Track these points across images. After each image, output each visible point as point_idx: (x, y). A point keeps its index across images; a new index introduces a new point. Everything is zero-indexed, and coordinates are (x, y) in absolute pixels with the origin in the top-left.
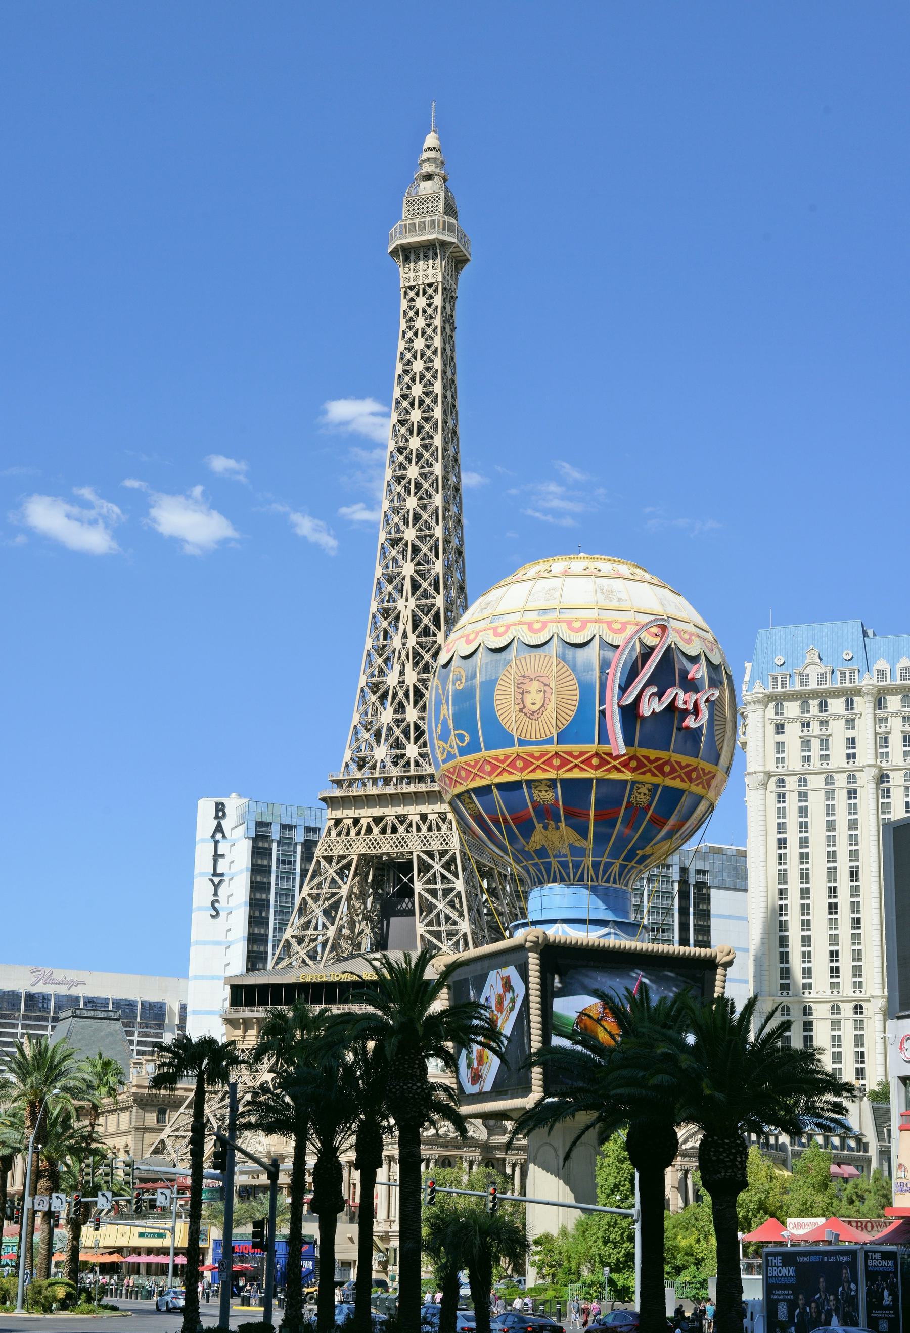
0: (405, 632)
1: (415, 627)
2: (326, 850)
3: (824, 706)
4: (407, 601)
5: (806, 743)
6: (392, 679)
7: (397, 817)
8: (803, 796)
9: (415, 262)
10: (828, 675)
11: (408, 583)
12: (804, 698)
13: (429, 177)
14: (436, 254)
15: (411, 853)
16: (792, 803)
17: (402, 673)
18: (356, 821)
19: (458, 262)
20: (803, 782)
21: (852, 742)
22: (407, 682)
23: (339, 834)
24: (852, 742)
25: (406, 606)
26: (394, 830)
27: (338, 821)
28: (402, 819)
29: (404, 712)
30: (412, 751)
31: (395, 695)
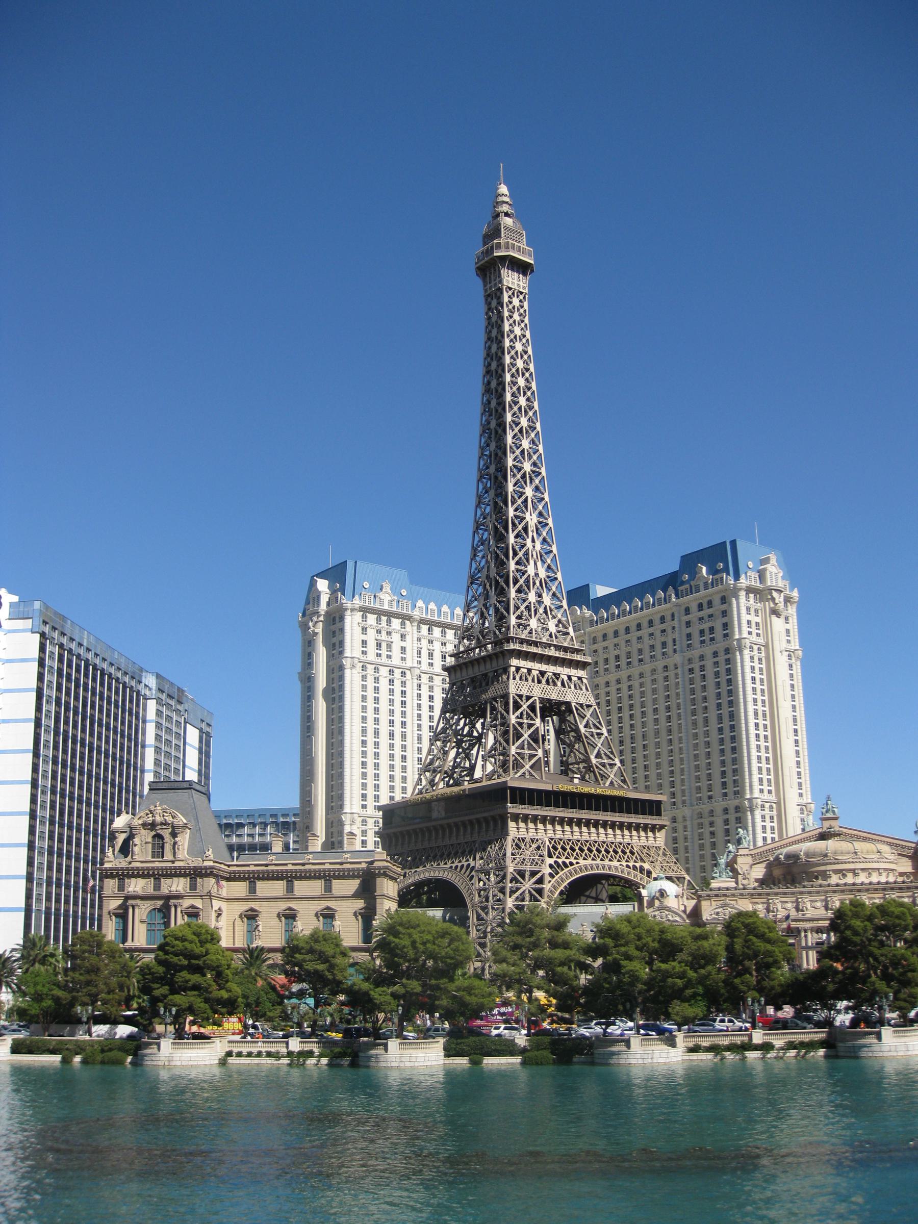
3: (389, 622)
5: (379, 645)
6: (531, 570)
7: (554, 674)
8: (376, 680)
10: (395, 603)
12: (379, 613)
13: (507, 214)
15: (568, 704)
16: (370, 684)
18: (529, 671)
20: (376, 670)
21: (403, 649)
24: (403, 649)
26: (555, 684)
28: (557, 676)
31: (534, 584)
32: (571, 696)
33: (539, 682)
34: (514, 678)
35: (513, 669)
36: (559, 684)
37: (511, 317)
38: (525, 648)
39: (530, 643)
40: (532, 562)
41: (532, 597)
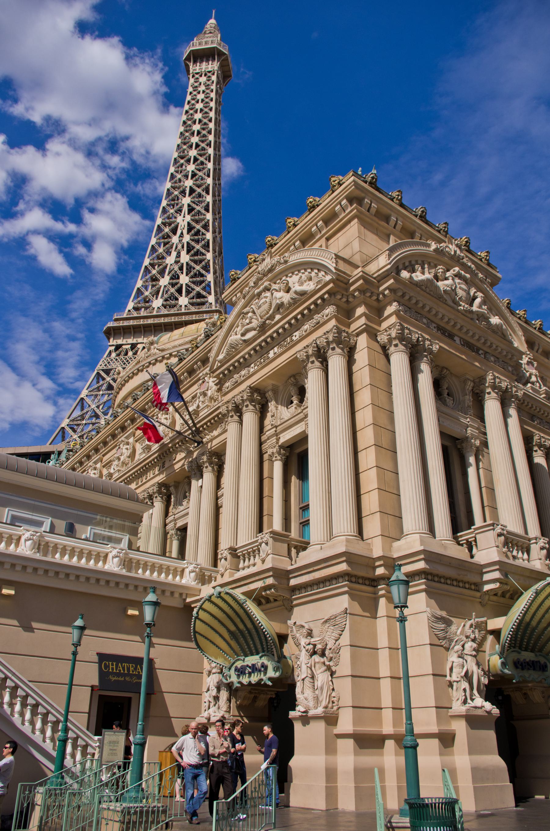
0: (182, 233)
1: (188, 232)
2: (106, 365)
4: (184, 217)
6: (170, 260)
9: (200, 63)
11: (185, 209)
14: (215, 59)
17: (178, 255)
18: (133, 346)
19: (225, 75)
22: (182, 261)
23: (118, 355)
25: (183, 220)
27: (118, 347)
29: (178, 278)
30: (183, 301)
40: (174, 254)
41: (164, 281)
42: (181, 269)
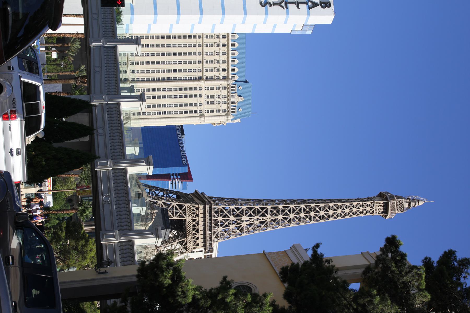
1: (261, 222)
6: (244, 218)
7: (198, 229)
11: (276, 217)
13: (410, 204)
15: (185, 237)
18: (197, 215)
23: (193, 210)
26: (194, 230)
27: (198, 209)
28: (198, 231)
30: (220, 229)
31: (238, 220)
32: (189, 238)
33: (194, 221)
34: (193, 207)
35: (197, 206)
36: (194, 232)
37: (360, 206)
38: (207, 214)
39: (210, 216)
40: (248, 218)
42: (239, 223)
